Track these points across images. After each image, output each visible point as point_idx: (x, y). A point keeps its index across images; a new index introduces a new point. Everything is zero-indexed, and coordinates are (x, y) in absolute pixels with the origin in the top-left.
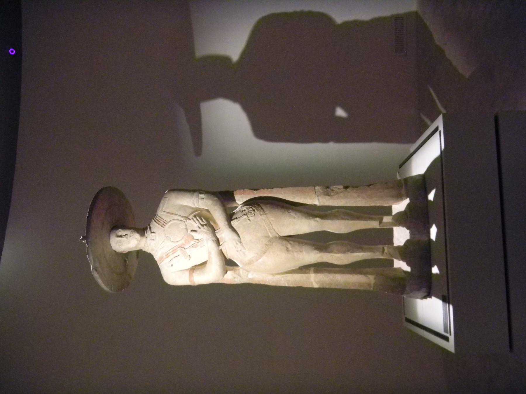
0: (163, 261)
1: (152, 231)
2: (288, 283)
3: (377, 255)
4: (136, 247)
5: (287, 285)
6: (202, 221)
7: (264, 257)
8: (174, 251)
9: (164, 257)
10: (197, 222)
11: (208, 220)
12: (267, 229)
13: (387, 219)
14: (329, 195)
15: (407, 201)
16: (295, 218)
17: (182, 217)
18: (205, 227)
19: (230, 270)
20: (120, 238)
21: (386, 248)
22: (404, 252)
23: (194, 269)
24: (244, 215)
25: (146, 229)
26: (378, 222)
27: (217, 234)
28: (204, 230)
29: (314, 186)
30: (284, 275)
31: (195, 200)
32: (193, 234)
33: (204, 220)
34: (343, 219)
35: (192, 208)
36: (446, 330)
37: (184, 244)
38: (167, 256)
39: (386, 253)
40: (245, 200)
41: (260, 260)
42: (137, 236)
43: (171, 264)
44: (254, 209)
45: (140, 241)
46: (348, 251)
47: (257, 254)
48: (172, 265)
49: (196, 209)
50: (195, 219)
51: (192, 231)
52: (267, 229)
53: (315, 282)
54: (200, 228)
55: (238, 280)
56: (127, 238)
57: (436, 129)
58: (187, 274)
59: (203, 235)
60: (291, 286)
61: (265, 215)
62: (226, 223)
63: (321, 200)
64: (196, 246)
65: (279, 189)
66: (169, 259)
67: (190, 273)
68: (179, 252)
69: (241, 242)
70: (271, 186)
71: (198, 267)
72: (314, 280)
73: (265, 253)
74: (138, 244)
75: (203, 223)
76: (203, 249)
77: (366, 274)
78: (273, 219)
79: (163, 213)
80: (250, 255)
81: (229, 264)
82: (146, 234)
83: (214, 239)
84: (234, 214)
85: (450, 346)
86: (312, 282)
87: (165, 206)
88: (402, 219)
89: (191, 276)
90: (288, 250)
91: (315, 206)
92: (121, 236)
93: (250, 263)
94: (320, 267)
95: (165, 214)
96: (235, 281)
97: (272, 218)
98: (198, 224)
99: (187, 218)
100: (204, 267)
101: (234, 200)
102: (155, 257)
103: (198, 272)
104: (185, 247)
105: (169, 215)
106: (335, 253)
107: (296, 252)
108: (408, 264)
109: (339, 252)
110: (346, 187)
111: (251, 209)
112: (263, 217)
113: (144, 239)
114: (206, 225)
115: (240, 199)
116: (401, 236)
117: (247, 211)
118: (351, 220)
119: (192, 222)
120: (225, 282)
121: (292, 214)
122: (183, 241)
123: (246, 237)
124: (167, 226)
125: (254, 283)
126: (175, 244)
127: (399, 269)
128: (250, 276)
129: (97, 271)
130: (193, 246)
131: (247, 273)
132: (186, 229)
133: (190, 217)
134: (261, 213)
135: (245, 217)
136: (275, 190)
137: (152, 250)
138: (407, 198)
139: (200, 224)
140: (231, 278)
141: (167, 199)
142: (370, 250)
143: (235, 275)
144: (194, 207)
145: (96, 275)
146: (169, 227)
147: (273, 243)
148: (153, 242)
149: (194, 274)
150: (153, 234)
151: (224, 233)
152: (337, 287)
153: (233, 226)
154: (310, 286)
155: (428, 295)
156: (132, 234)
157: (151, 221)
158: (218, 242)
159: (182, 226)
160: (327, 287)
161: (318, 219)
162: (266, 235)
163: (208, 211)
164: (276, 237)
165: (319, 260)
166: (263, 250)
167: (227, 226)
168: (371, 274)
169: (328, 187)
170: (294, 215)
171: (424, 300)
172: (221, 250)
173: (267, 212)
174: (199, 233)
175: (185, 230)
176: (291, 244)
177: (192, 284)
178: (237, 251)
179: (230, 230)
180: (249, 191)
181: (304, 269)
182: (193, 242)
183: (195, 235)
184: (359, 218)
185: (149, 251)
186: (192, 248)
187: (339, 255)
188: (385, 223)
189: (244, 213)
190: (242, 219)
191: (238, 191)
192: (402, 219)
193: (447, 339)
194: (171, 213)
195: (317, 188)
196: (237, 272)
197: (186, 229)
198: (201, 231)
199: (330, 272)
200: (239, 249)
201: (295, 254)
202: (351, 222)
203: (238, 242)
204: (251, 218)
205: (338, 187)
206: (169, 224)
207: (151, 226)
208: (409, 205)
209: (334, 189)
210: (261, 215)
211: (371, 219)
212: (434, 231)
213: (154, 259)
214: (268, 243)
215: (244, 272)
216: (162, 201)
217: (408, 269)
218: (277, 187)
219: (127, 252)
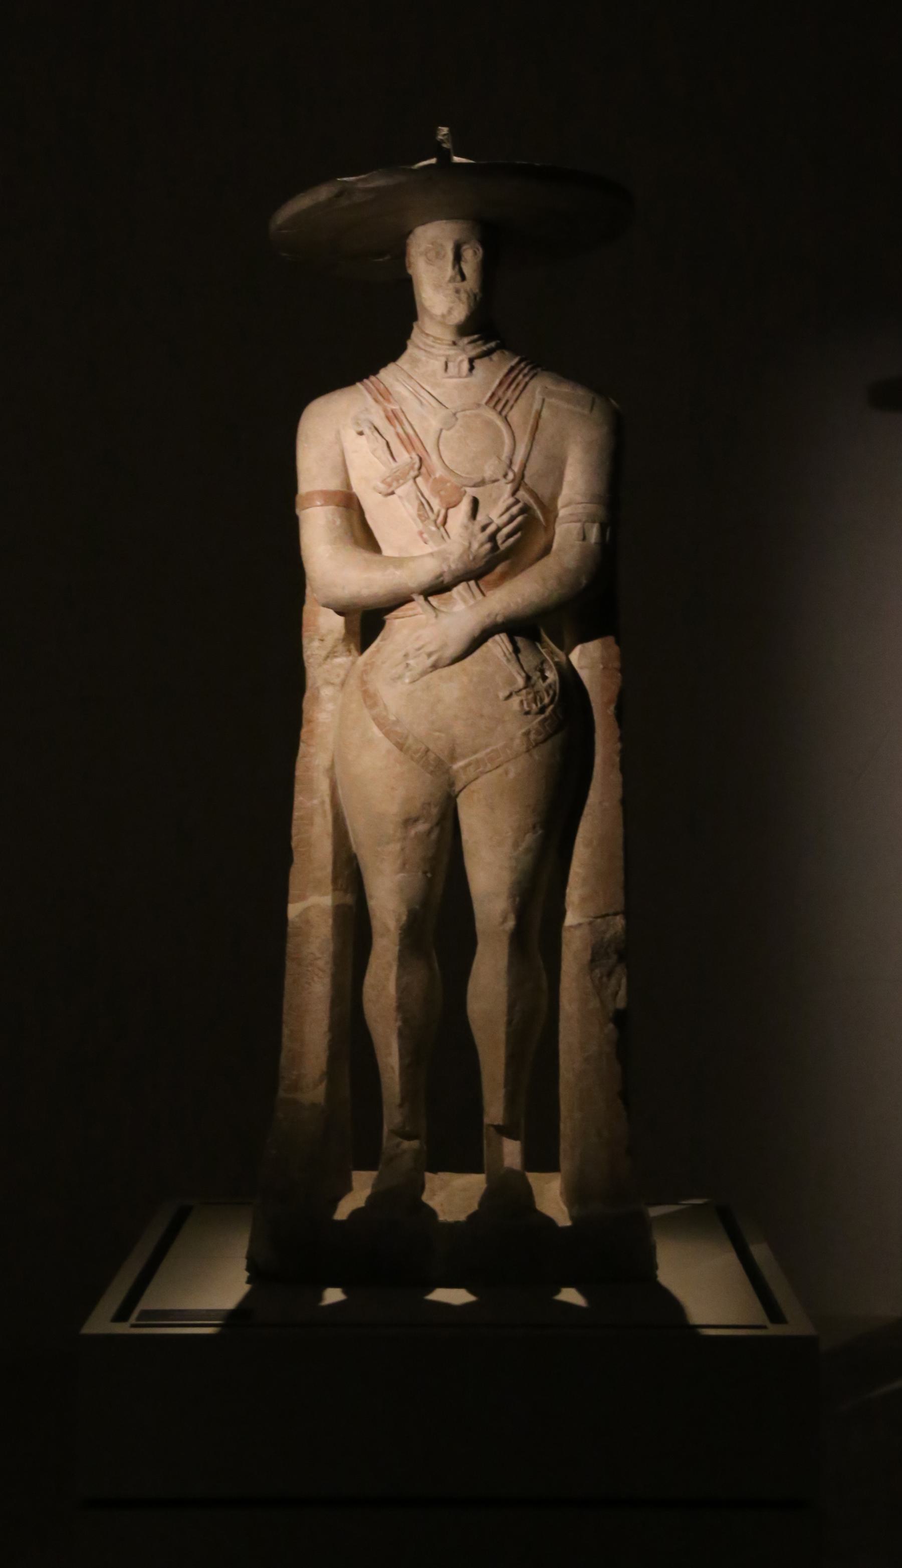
0: (376, 401)
1: (477, 363)
2: (301, 818)
3: (393, 1114)
4: (425, 309)
5: (296, 814)
6: (509, 536)
7: (386, 745)
8: (409, 442)
9: (390, 407)
10: (506, 517)
11: (511, 552)
12: (478, 756)
13: (512, 1152)
14: (593, 960)
15: (563, 1219)
16: (516, 845)
17: (524, 466)
18: (488, 546)
19: (347, 624)
20: (450, 256)
21: (415, 1144)
22: (401, 1203)
23: (349, 504)
24: (528, 678)
25: (486, 339)
26: (499, 1121)
27: (461, 587)
28: (475, 545)
29: (627, 913)
30: (328, 806)
31: (579, 509)
32: (465, 506)
33: (512, 540)
34: (511, 1007)
35: (555, 497)
36: (147, 1315)
37: (429, 474)
38: (393, 417)
39: (398, 1145)
40: (585, 675)
41: (376, 732)
42: (460, 314)
43: (367, 431)
44: (549, 711)
46: (405, 1021)
47: (397, 722)
48: (361, 433)
49: (550, 510)
50: (515, 510)
51: (475, 503)
52: (478, 756)
53: (307, 909)
54: (484, 528)
55: (314, 650)
56: (452, 280)
57: (774, 1313)
58: (334, 485)
59: (459, 540)
60: (294, 831)
61: (524, 748)
62: (500, 619)
63: (578, 933)
64: (423, 517)
65: (618, 793)
66: (382, 424)
67: (335, 493)
68: (404, 457)
69: (435, 667)
70: (628, 764)
71: (355, 519)
72: (311, 905)
73: (400, 746)
74: (432, 317)
76: (415, 541)
77: (331, 1073)
78: (512, 775)
79: (538, 397)
80: (394, 696)
81: (367, 623)
82: (466, 340)
83: (447, 579)
84: (534, 637)
85: (101, 1323)
86: (302, 898)
87: (565, 406)
88: (508, 1201)
89: (328, 497)
90: (409, 822)
91: (562, 914)
92: (458, 258)
93: (369, 698)
94: (354, 924)
95: (536, 406)
96: (312, 640)
97: (513, 771)
98: (498, 521)
99: (519, 483)
100: (356, 543)
101: (584, 638)
102: (391, 367)
103: (338, 522)
104: (419, 480)
105: (531, 422)
106: (399, 979)
107: (403, 849)
108: (356, 1214)
109: (403, 990)
110: (620, 1019)
112: (517, 741)
113: (449, 337)
114: (495, 547)
115: (586, 659)
116: (453, 1196)
117: (541, 685)
118: (509, 1035)
119: (506, 499)
120: (307, 607)
121: (529, 838)
122: (439, 472)
123: (452, 686)
124: (491, 415)
125: (306, 705)
126: (430, 445)
127: (346, 1188)
128: (326, 692)
129: (340, 195)
130: (424, 506)
131: (338, 681)
132: (482, 483)
133: (522, 494)
134: (532, 736)
135: (520, 682)
136: (616, 777)
137: (415, 361)
138: (572, 1218)
139: (499, 529)
140: (323, 627)
141: (586, 412)
142: (408, 1095)
143: (330, 641)
144: (561, 502)
145: (323, 193)
146: (489, 423)
147: (431, 773)
148: (438, 365)
149: (331, 508)
150: (465, 366)
151: (465, 611)
152: (288, 981)
153: (490, 643)
154: (293, 892)
155: (257, 1272)
156: (464, 296)
157: (515, 352)
158: (437, 589)
159: (490, 469)
160: (290, 947)
161: (511, 924)
162: (459, 750)
163: (547, 550)
164: (452, 784)
165: (376, 924)
166: (410, 741)
167: (488, 621)
168: (331, 1094)
169: (622, 957)
170: (523, 846)
171: (243, 1263)
172: (410, 600)
173: (536, 755)
174: (466, 527)
175: (477, 478)
176: (429, 832)
177: (299, 500)
178: (406, 656)
179: (477, 633)
180: (614, 689)
181: (349, 874)
182: (436, 504)
183: (460, 514)
184: (514, 1059)
185: (411, 350)
186: (416, 503)
187: (392, 988)
188: (500, 1144)
189: (536, 676)
190: (513, 668)
191: (615, 650)
192: (508, 1201)
193: (122, 1315)
194: (536, 428)
195: (619, 922)
196: (341, 648)
197: (482, 483)
198: (473, 535)
199: (338, 959)
200: (411, 662)
201: (396, 847)
202: (501, 1034)
203: (433, 658)
204: (515, 701)
205: (622, 992)
206: (499, 423)
207: (495, 357)
208: (549, 1222)
209: (613, 981)
210: (527, 734)
211: (511, 1100)
212: (458, 1297)
213: (384, 365)
214: (432, 756)
215: (342, 673)
216: (580, 392)
217: (344, 1210)
218: (625, 785)
219: (410, 272)
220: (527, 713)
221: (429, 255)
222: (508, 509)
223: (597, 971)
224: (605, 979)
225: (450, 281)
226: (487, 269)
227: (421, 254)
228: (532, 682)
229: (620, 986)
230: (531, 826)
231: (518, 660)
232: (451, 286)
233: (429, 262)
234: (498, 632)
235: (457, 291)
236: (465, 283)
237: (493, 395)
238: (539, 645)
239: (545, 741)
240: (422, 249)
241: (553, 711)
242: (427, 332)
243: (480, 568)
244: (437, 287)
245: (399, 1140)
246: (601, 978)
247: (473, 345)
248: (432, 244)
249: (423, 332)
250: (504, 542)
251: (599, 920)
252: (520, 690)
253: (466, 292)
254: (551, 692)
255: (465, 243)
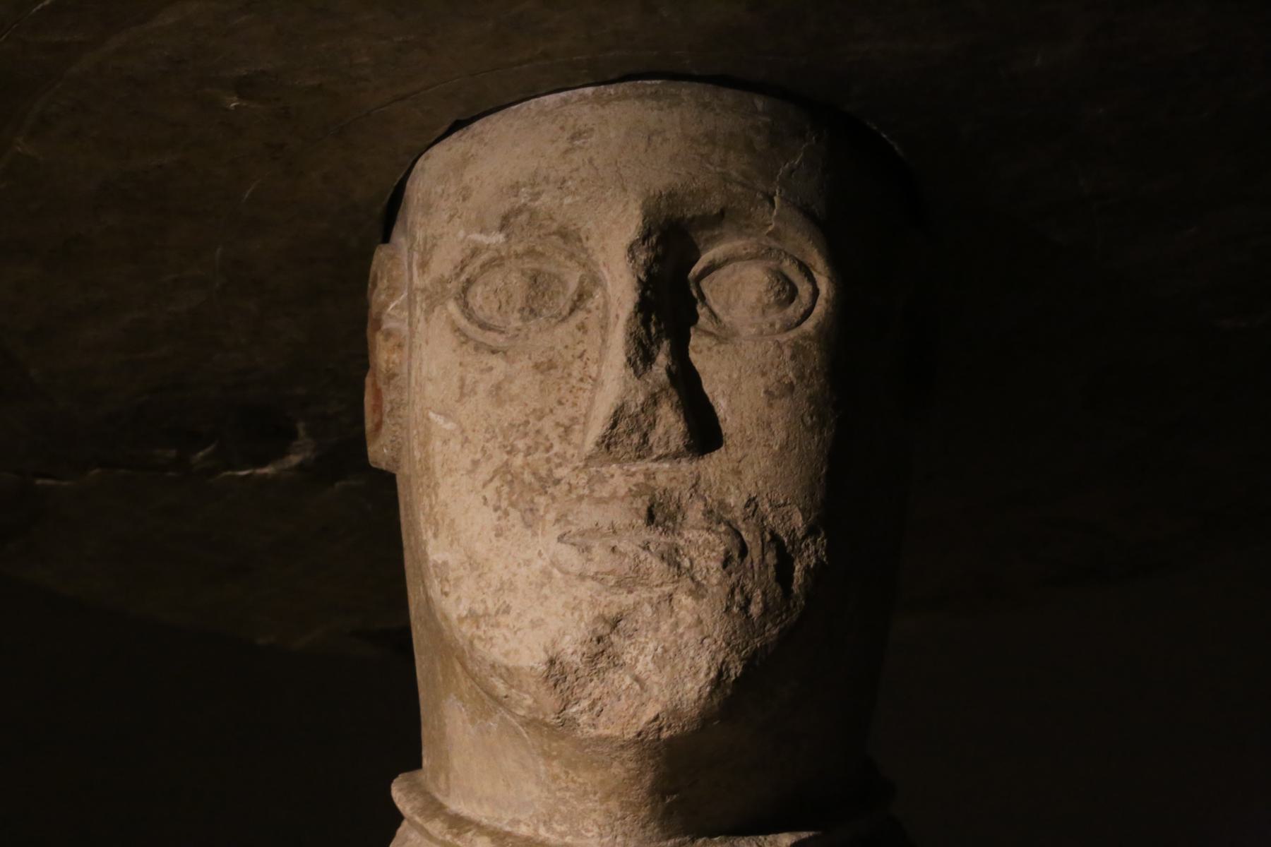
4: (449, 651)
20: (620, 290)
42: (671, 664)
45: (553, 731)
56: (625, 434)
74: (488, 702)
92: (668, 307)
156: (703, 546)
219: (379, 452)
221: (478, 296)
225: (607, 443)
226: (864, 389)
227: (434, 299)
232: (619, 478)
233: (478, 334)
235: (658, 513)
236: (712, 466)
240: (442, 264)
242: (456, 805)
244: (524, 491)
248: (505, 223)
249: (434, 808)
253: (715, 515)
255: (717, 220)
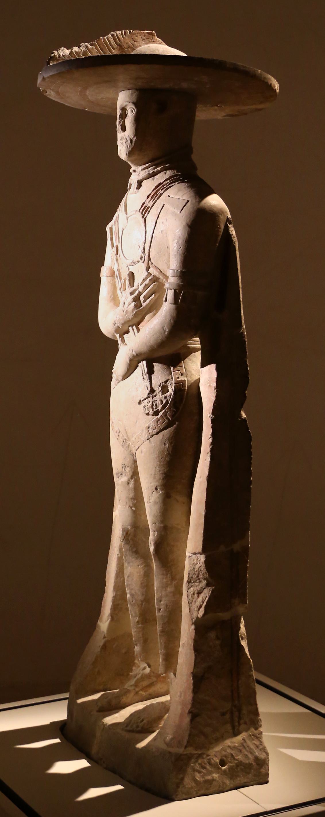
6: (146, 298)
24: (152, 391)
39: (144, 668)
61: (146, 437)
75: (142, 298)
111: (160, 407)
134: (150, 430)
139: (140, 294)
189: (158, 389)
197: (133, 264)
204: (143, 405)
220: (148, 414)
222: (144, 280)
223: (192, 589)
224: (196, 595)
228: (155, 394)
229: (203, 602)
230: (154, 488)
231: (150, 379)
234: (143, 361)
237: (144, 204)
238: (172, 368)
239: (157, 433)
241: (165, 414)
243: (132, 319)
245: (146, 665)
246: (194, 594)
247: (146, 170)
250: (144, 302)
251: (194, 556)
252: (145, 399)
254: (164, 402)
